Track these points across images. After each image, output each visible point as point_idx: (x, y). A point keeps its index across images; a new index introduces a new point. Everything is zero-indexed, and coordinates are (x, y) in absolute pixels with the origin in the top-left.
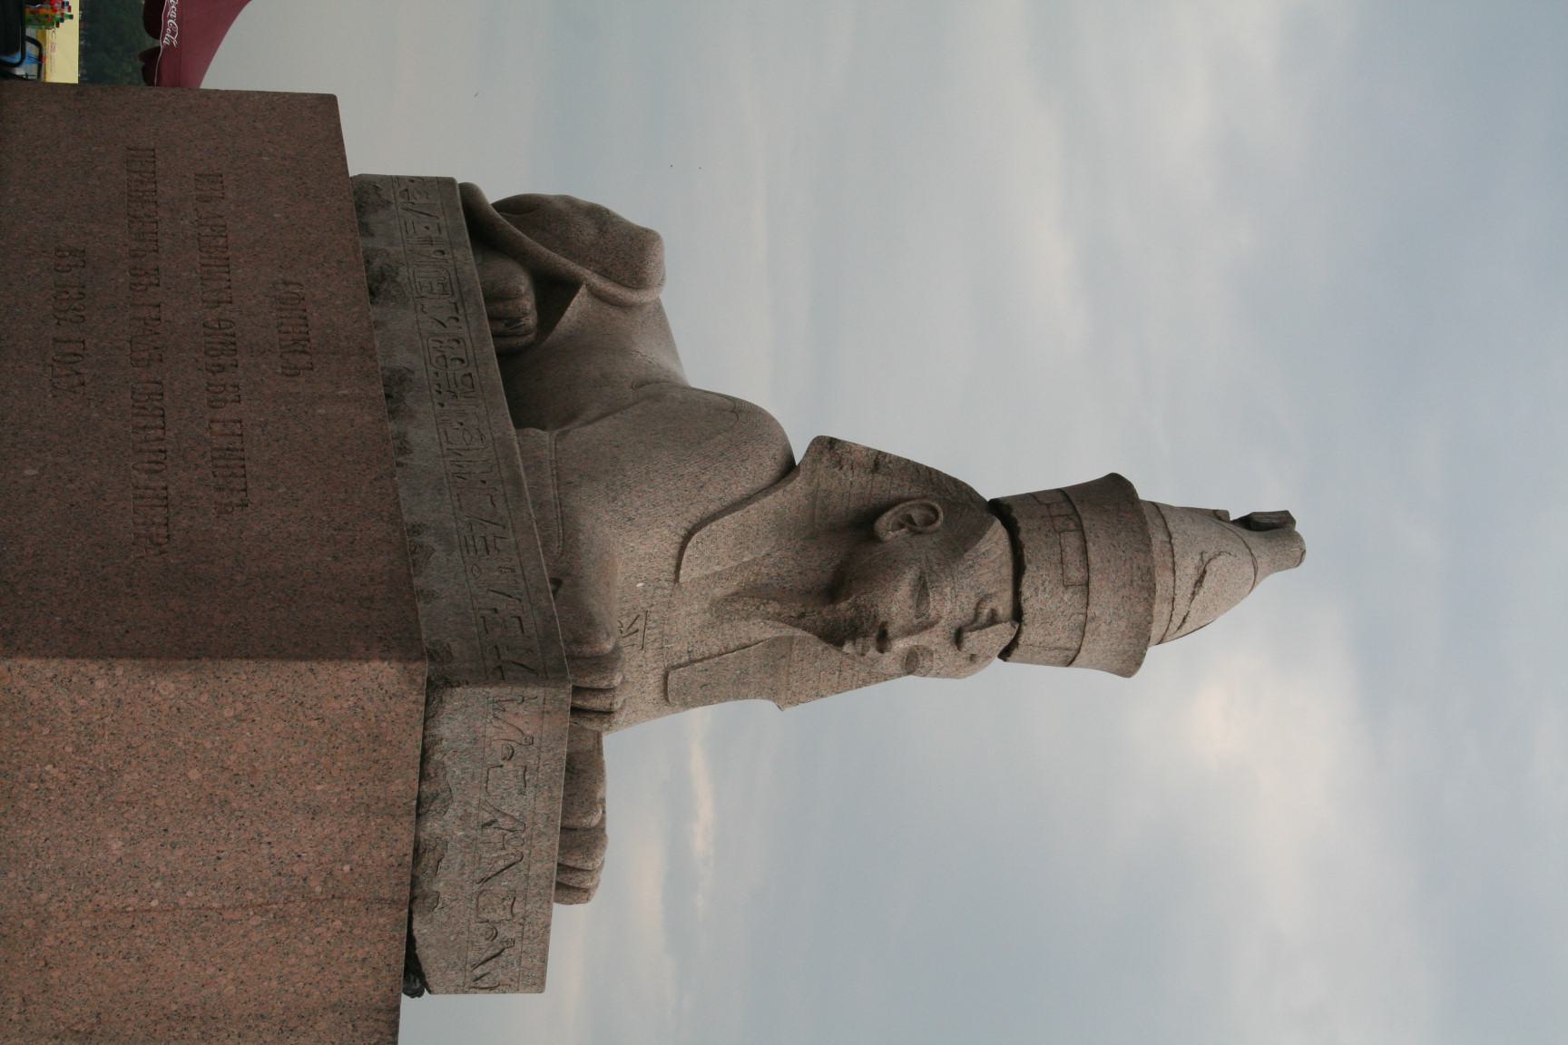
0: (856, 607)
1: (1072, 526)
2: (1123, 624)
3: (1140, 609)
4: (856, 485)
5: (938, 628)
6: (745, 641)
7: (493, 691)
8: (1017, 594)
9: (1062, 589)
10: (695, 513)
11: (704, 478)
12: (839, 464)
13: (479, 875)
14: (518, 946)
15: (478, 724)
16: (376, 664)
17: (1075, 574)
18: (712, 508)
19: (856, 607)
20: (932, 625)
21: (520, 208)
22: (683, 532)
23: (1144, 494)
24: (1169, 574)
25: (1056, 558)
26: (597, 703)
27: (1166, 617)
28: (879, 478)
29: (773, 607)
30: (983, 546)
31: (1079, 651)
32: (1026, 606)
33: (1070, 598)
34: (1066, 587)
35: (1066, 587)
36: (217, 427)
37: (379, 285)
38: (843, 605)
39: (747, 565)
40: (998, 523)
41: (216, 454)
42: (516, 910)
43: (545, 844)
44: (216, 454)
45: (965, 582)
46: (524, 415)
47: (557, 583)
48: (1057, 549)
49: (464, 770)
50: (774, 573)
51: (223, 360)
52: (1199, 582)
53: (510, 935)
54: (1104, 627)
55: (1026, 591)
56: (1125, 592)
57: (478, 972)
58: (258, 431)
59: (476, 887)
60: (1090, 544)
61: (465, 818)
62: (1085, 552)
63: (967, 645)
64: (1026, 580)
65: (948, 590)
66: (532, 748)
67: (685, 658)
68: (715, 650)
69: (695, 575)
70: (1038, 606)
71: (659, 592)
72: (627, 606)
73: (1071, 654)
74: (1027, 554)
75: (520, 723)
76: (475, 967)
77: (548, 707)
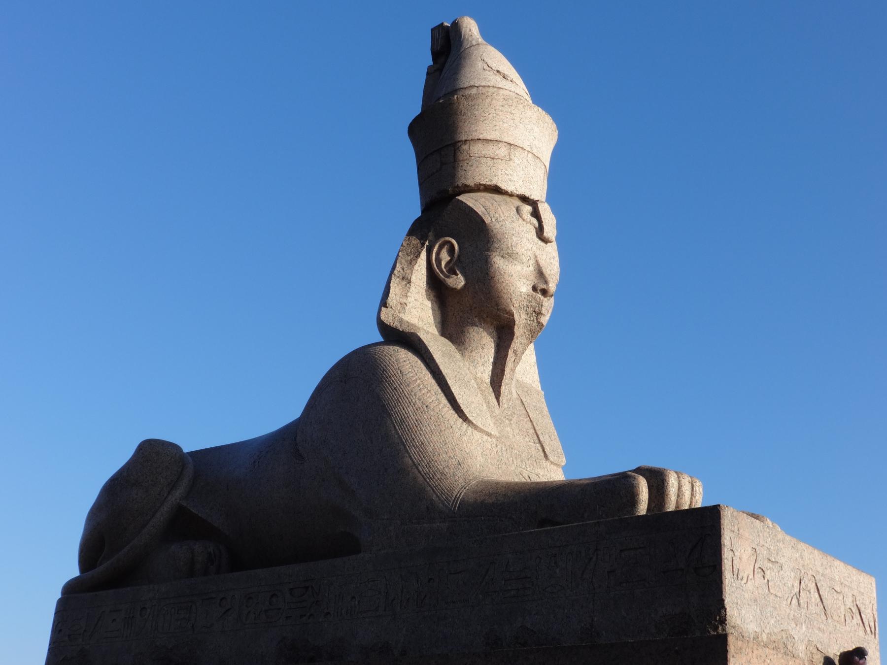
1: (465, 147)
2: (536, 129)
4: (417, 296)
8: (511, 195)
9: (511, 163)
11: (419, 404)
13: (824, 618)
15: (746, 595)
17: (502, 151)
18: (444, 400)
21: (92, 551)
22: (465, 425)
23: (418, 110)
25: (490, 162)
28: (413, 278)
30: (479, 210)
33: (518, 158)
34: (510, 160)
35: (510, 160)
38: (516, 317)
40: (463, 198)
43: (806, 554)
46: (347, 546)
47: (543, 523)
48: (483, 160)
49: (772, 616)
50: (481, 368)
54: (536, 142)
57: (868, 629)
59: (830, 621)
60: (481, 137)
62: (487, 141)
64: (503, 186)
66: (758, 552)
67: (538, 445)
68: (530, 424)
70: (521, 183)
76: (865, 631)
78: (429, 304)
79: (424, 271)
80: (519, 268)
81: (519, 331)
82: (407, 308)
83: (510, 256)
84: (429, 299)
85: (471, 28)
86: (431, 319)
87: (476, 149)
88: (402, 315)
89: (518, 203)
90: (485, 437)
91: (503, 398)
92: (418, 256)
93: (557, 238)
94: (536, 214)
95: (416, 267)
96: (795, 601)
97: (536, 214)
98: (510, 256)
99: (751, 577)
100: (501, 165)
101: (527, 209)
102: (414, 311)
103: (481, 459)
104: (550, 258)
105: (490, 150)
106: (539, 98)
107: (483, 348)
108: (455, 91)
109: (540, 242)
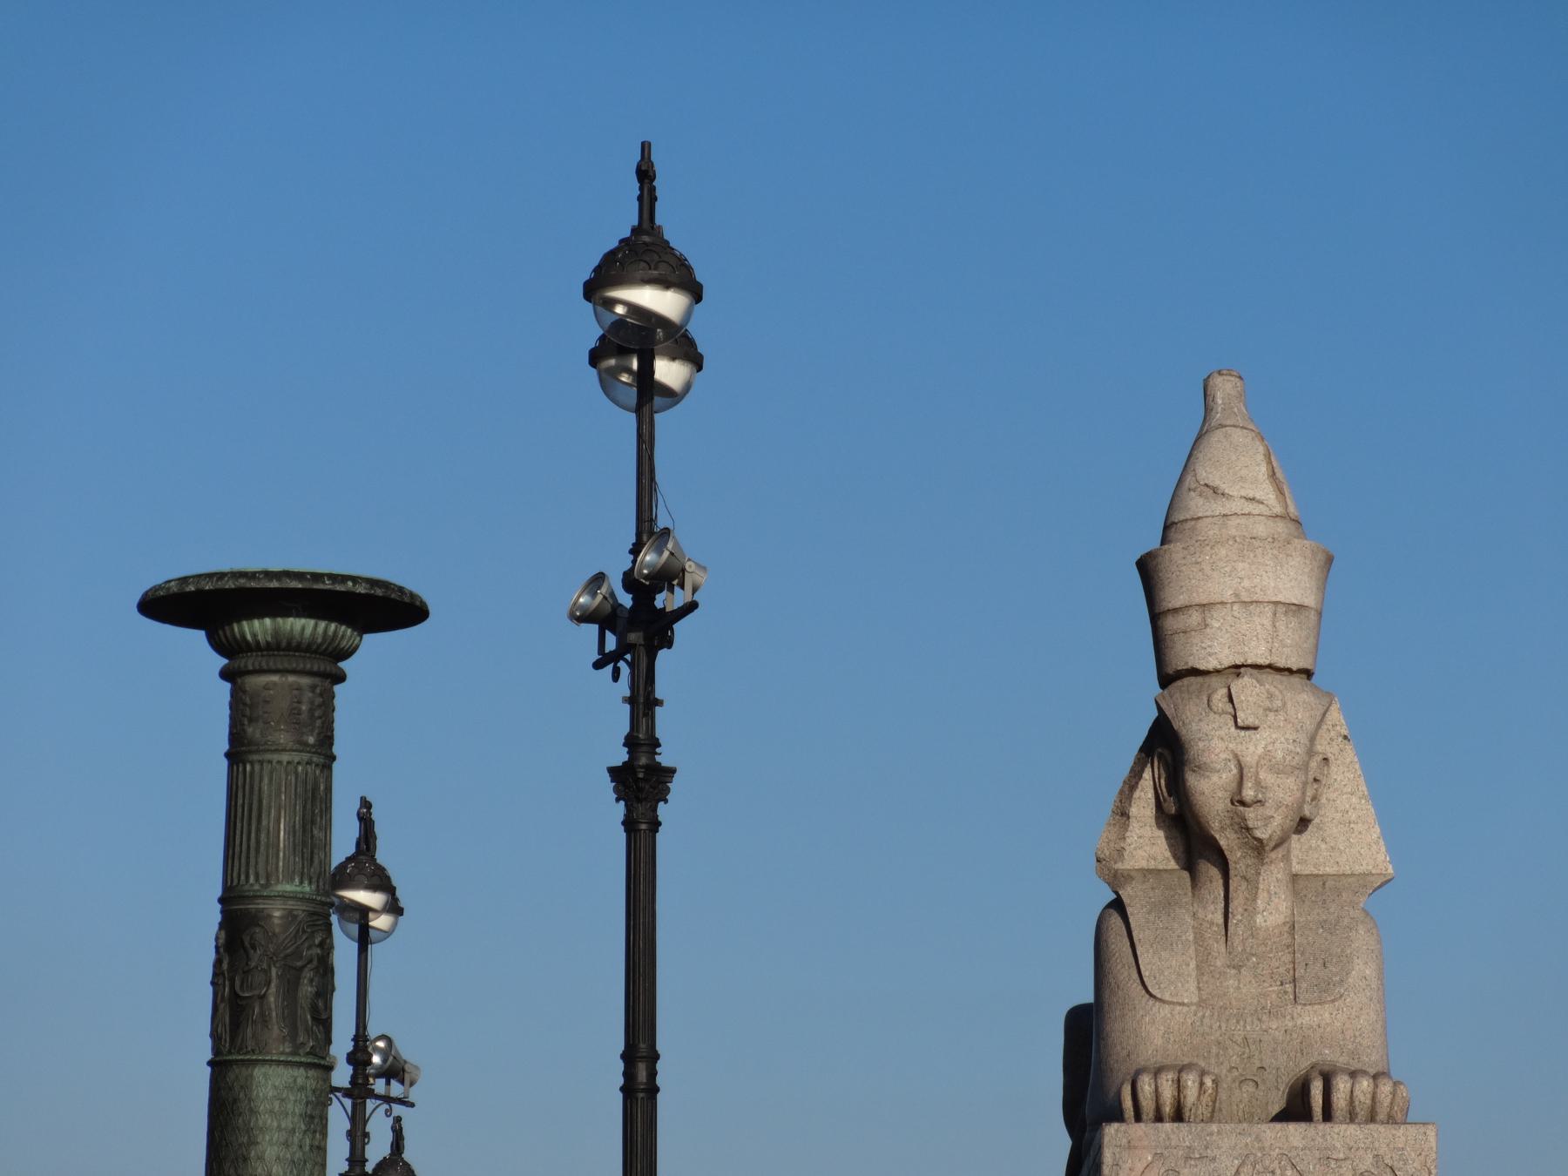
0: (1222, 829)
2: (1240, 565)
3: (1223, 552)
5: (1239, 749)
6: (1286, 928)
8: (1218, 671)
12: (1121, 851)
14: (1381, 1152)
17: (1195, 618)
18: (1135, 975)
19: (1222, 829)
20: (1236, 756)
22: (1151, 1002)
24: (1200, 524)
26: (1168, 1093)
27: (1243, 520)
28: (1134, 811)
29: (1237, 904)
31: (1276, 603)
32: (1226, 663)
34: (1206, 626)
35: (1206, 626)
38: (1223, 843)
39: (1199, 938)
42: (1341, 1156)
45: (1194, 727)
48: (1176, 638)
52: (1215, 490)
53: (1369, 1159)
54: (1246, 583)
55: (1211, 664)
56: (1207, 569)
60: (1170, 606)
62: (1176, 610)
63: (1250, 721)
64: (1202, 667)
65: (1201, 745)
67: (1289, 988)
68: (1288, 958)
69: (1192, 986)
70: (1227, 651)
71: (1206, 1021)
72: (1214, 1050)
73: (1281, 609)
75: (1140, 1166)
77: (1125, 1141)
78: (1161, 833)
79: (1151, 794)
80: (1215, 778)
82: (1126, 854)
83: (1200, 768)
84: (1159, 827)
85: (1225, 389)
86: (1168, 854)
88: (1119, 866)
90: (1179, 1008)
91: (1236, 941)
95: (1137, 794)
98: (1200, 768)
100: (1196, 639)
102: (1141, 852)
103: (1159, 1041)
109: (1242, 733)
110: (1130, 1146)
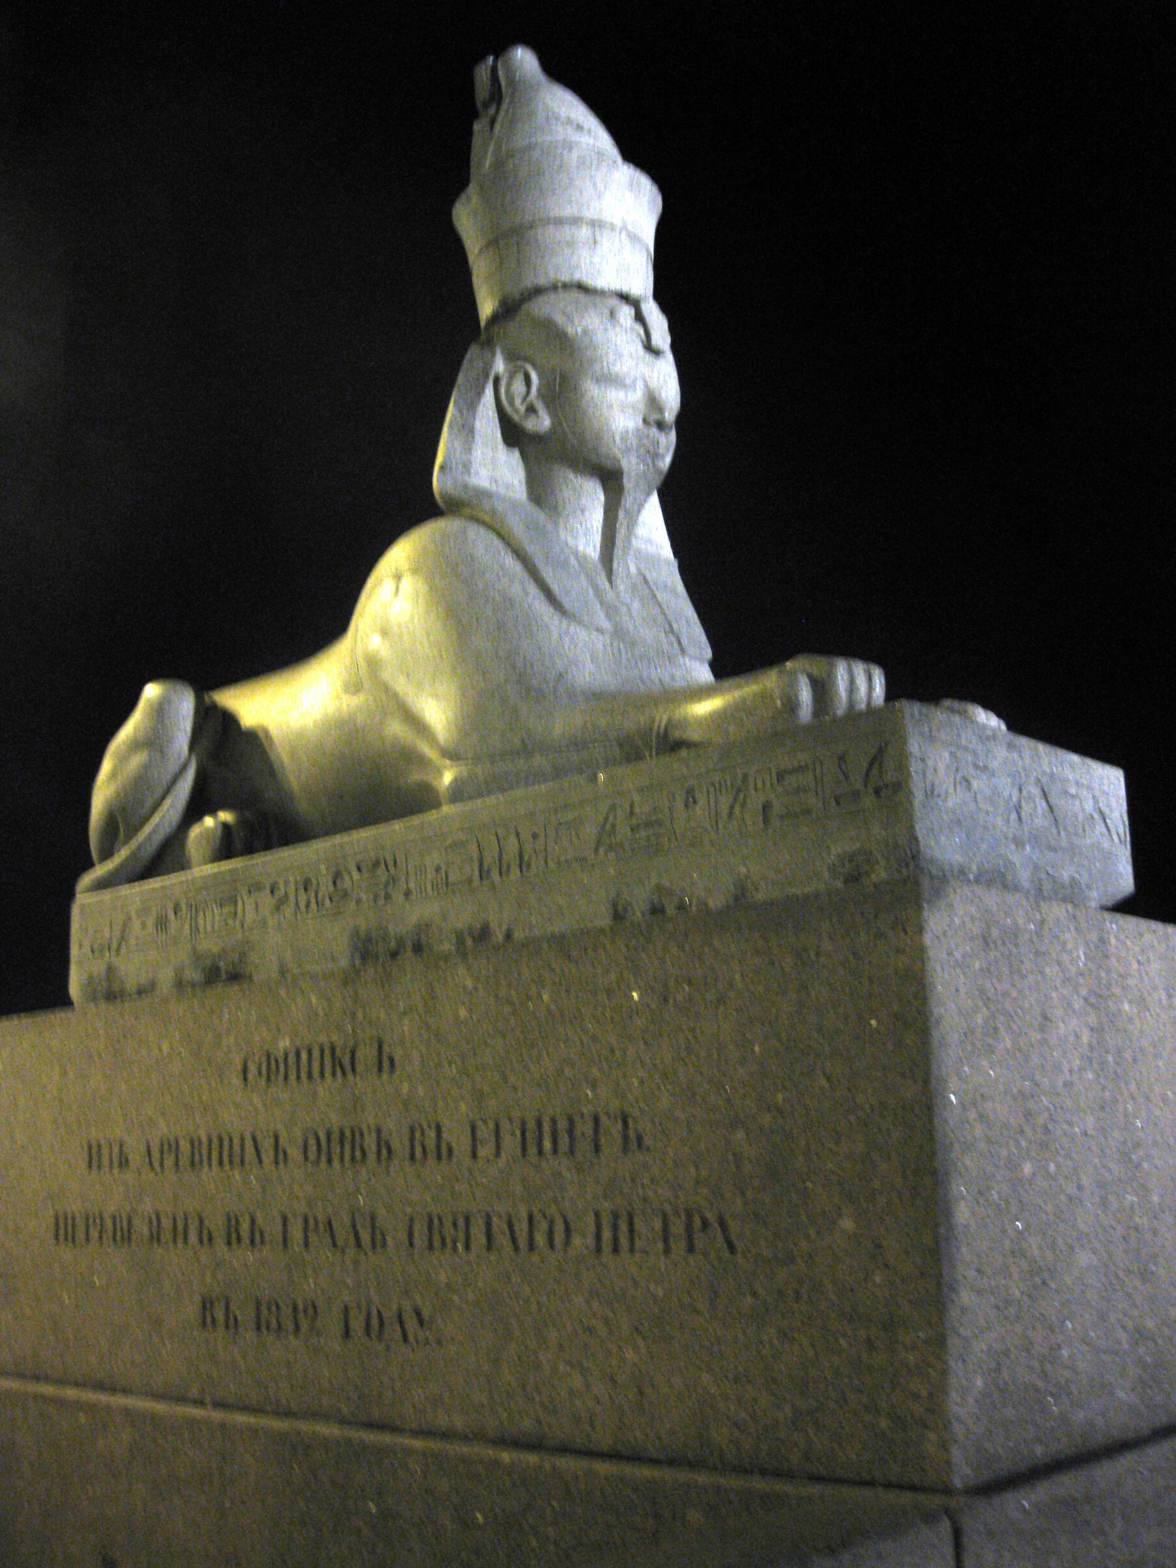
0: (627, 450)
1: (532, 233)
5: (647, 371)
7: (918, 796)
10: (541, 607)
16: (927, 939)
17: (584, 232)
18: (533, 590)
30: (559, 319)
36: (482, 1152)
37: (223, 974)
41: (532, 1150)
44: (532, 1150)
51: (370, 1142)
56: (600, 186)
58: (493, 1103)
61: (1019, 843)
64: (590, 282)
74: (565, 277)
81: (628, 483)
87: (548, 234)
89: (615, 302)
92: (480, 393)
93: (674, 347)
94: (639, 317)
95: (481, 408)
96: (1014, 816)
97: (639, 317)
98: (610, 380)
99: (951, 790)
101: (626, 313)
104: (665, 379)
105: (567, 232)
106: (632, 152)
107: (583, 511)
108: (510, 155)
110: (931, 739)
